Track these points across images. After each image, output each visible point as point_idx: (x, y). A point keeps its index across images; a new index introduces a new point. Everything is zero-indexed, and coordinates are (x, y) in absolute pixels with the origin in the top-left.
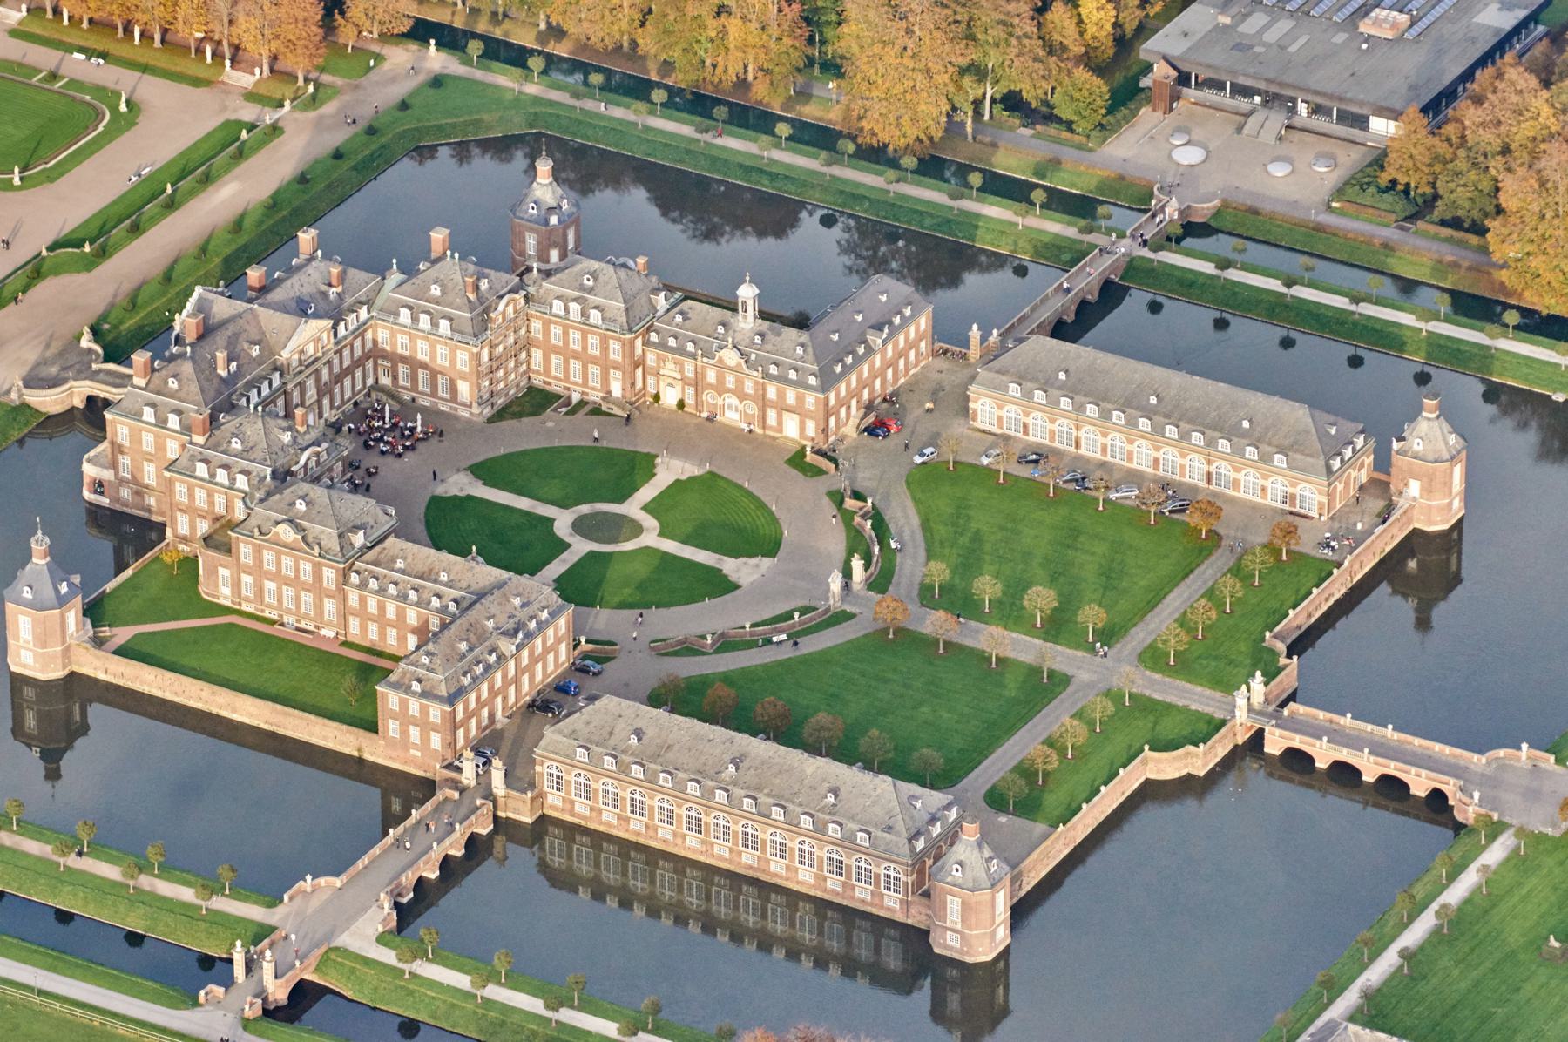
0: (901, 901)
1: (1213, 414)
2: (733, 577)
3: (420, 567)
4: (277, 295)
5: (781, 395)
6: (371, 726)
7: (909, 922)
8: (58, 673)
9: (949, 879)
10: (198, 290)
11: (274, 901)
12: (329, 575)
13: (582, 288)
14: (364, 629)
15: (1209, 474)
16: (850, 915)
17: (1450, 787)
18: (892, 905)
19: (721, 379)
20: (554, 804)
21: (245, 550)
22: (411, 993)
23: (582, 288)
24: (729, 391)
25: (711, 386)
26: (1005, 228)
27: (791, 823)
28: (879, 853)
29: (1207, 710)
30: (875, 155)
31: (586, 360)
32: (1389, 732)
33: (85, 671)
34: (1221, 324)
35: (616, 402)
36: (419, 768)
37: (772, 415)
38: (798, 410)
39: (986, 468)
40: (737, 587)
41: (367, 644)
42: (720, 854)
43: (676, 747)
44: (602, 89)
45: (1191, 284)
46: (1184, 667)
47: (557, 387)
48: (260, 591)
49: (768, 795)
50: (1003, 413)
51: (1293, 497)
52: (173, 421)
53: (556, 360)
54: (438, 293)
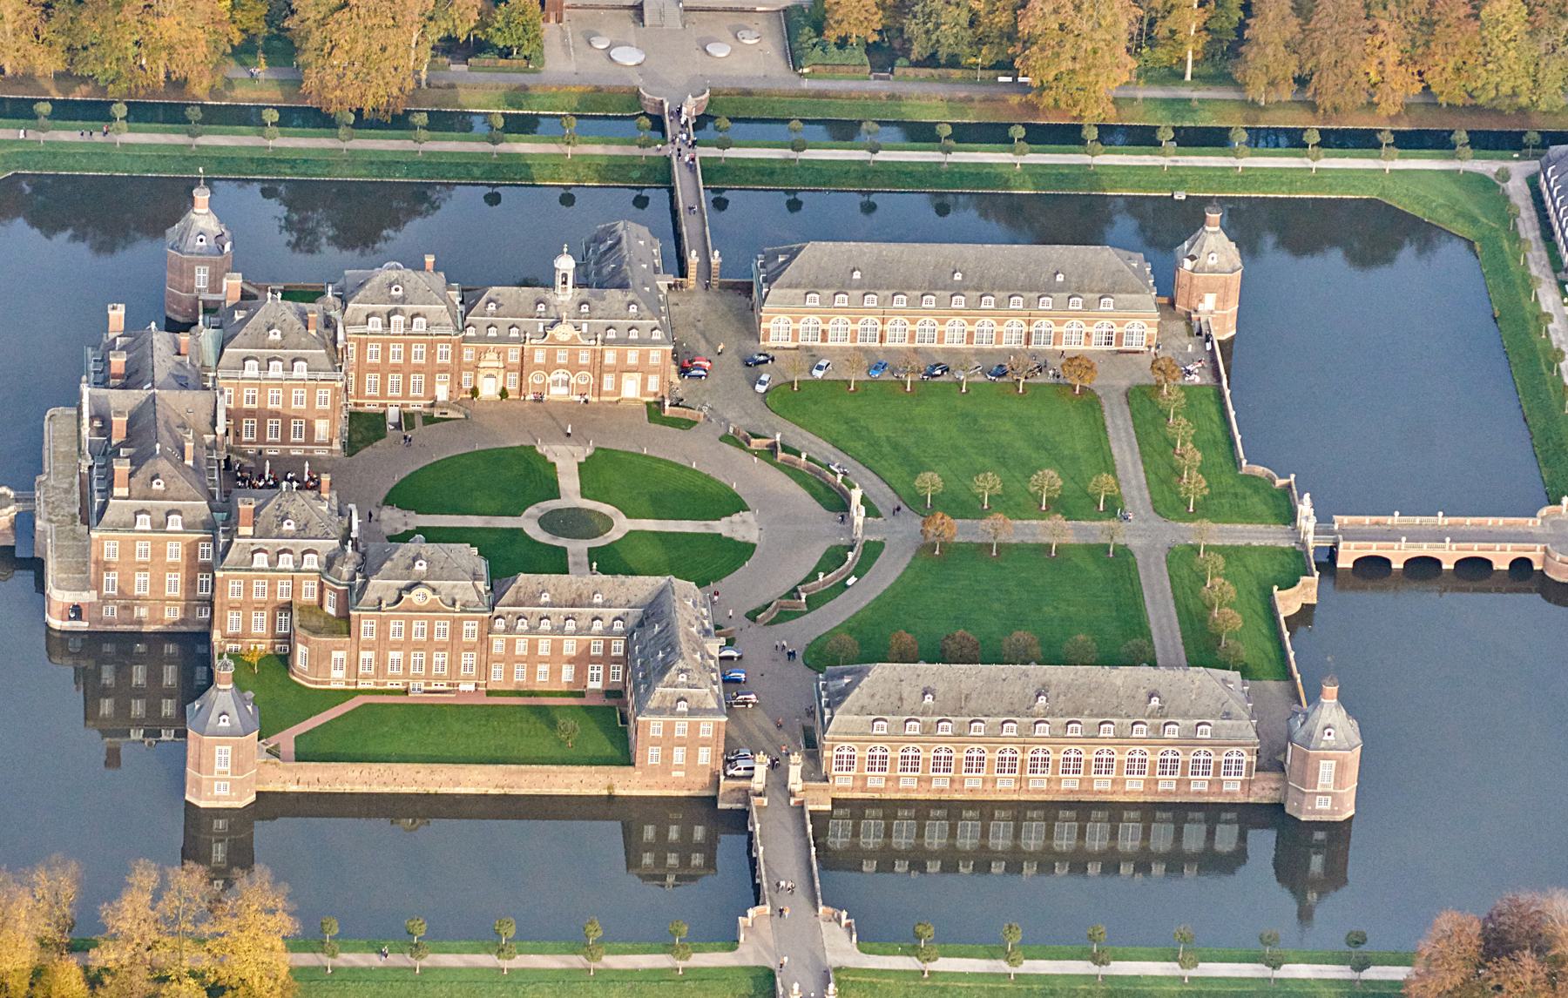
0: (1243, 782)
1: (1022, 276)
2: (738, 537)
3: (568, 596)
4: (160, 375)
5: (622, 358)
6: (625, 757)
7: (1251, 800)
8: (253, 798)
9: (1323, 745)
10: (86, 390)
11: (732, 943)
12: (471, 628)
13: (394, 300)
14: (509, 673)
15: (1029, 334)
16: (1180, 812)
17: (1535, 555)
18: (1233, 788)
19: (551, 357)
20: (844, 784)
21: (366, 624)
22: (944, 990)
23: (394, 300)
24: (561, 366)
25: (539, 367)
26: (557, 162)
27: (1122, 738)
28: (1217, 744)
29: (1270, 542)
30: (363, 122)
31: (406, 370)
32: (1441, 520)
33: (270, 788)
34: (794, 206)
35: (446, 405)
36: (682, 788)
37: (608, 382)
38: (643, 369)
39: (823, 381)
40: (754, 546)
41: (512, 688)
42: (1038, 787)
43: (974, 695)
44: (53, 116)
45: (772, 173)
46: (1205, 510)
47: (371, 406)
48: (381, 665)
49: (1090, 716)
50: (800, 326)
51: (1120, 336)
52: (175, 523)
53: (371, 379)
54: (278, 337)
